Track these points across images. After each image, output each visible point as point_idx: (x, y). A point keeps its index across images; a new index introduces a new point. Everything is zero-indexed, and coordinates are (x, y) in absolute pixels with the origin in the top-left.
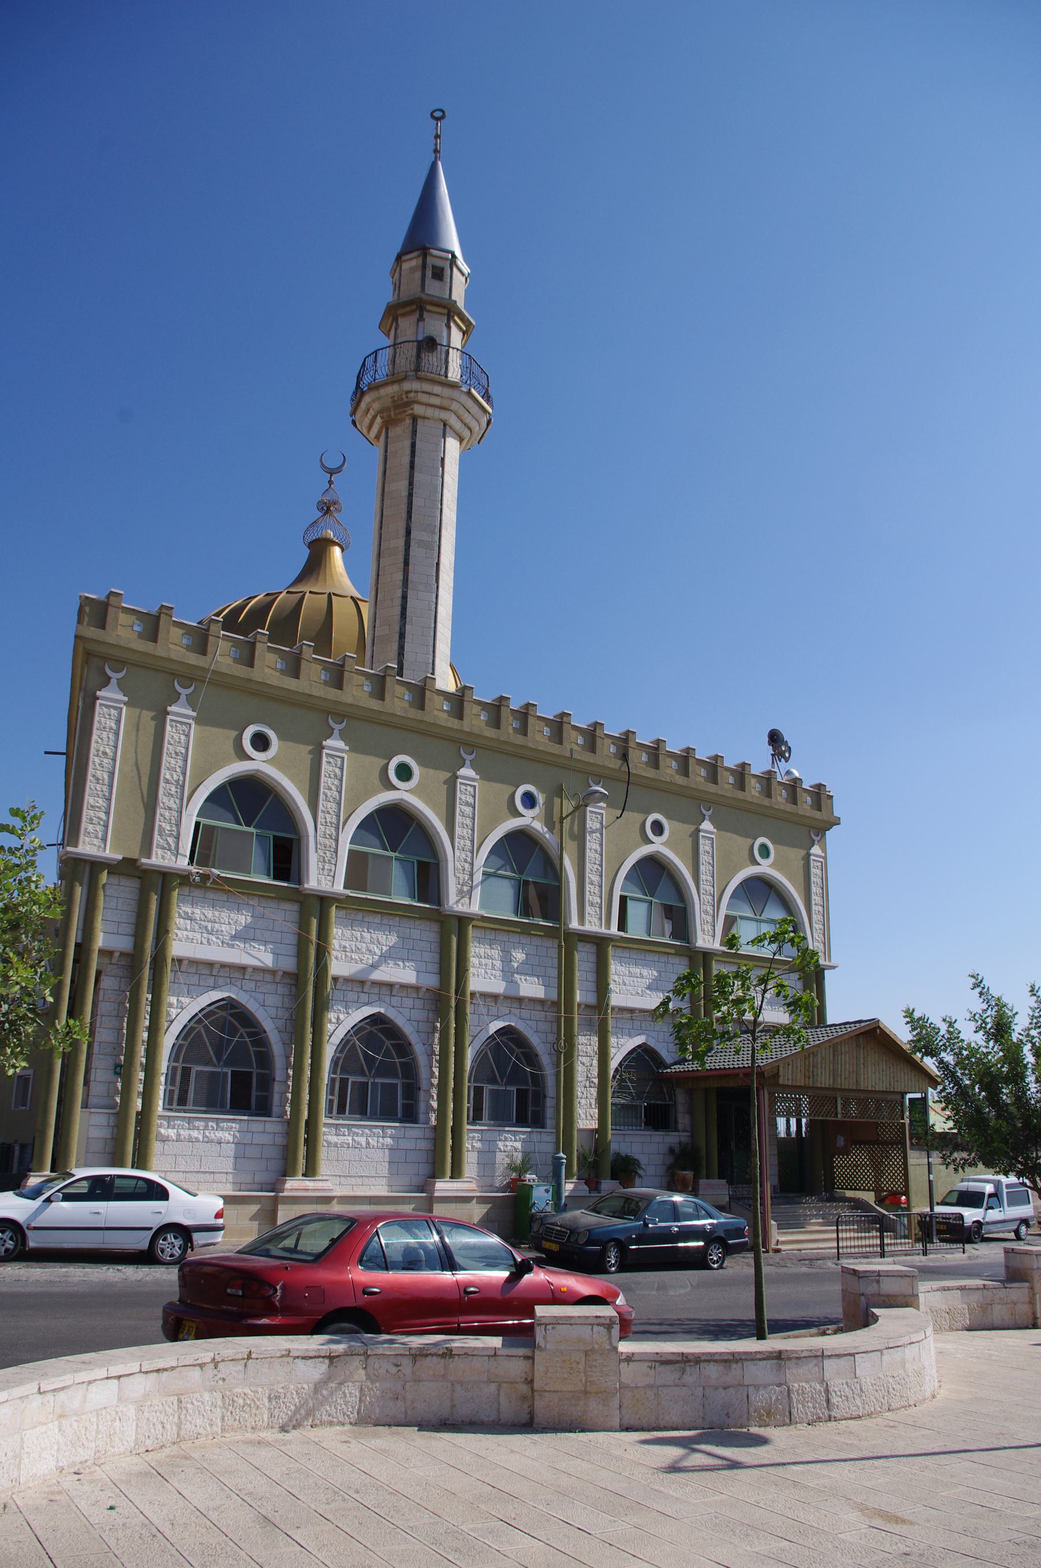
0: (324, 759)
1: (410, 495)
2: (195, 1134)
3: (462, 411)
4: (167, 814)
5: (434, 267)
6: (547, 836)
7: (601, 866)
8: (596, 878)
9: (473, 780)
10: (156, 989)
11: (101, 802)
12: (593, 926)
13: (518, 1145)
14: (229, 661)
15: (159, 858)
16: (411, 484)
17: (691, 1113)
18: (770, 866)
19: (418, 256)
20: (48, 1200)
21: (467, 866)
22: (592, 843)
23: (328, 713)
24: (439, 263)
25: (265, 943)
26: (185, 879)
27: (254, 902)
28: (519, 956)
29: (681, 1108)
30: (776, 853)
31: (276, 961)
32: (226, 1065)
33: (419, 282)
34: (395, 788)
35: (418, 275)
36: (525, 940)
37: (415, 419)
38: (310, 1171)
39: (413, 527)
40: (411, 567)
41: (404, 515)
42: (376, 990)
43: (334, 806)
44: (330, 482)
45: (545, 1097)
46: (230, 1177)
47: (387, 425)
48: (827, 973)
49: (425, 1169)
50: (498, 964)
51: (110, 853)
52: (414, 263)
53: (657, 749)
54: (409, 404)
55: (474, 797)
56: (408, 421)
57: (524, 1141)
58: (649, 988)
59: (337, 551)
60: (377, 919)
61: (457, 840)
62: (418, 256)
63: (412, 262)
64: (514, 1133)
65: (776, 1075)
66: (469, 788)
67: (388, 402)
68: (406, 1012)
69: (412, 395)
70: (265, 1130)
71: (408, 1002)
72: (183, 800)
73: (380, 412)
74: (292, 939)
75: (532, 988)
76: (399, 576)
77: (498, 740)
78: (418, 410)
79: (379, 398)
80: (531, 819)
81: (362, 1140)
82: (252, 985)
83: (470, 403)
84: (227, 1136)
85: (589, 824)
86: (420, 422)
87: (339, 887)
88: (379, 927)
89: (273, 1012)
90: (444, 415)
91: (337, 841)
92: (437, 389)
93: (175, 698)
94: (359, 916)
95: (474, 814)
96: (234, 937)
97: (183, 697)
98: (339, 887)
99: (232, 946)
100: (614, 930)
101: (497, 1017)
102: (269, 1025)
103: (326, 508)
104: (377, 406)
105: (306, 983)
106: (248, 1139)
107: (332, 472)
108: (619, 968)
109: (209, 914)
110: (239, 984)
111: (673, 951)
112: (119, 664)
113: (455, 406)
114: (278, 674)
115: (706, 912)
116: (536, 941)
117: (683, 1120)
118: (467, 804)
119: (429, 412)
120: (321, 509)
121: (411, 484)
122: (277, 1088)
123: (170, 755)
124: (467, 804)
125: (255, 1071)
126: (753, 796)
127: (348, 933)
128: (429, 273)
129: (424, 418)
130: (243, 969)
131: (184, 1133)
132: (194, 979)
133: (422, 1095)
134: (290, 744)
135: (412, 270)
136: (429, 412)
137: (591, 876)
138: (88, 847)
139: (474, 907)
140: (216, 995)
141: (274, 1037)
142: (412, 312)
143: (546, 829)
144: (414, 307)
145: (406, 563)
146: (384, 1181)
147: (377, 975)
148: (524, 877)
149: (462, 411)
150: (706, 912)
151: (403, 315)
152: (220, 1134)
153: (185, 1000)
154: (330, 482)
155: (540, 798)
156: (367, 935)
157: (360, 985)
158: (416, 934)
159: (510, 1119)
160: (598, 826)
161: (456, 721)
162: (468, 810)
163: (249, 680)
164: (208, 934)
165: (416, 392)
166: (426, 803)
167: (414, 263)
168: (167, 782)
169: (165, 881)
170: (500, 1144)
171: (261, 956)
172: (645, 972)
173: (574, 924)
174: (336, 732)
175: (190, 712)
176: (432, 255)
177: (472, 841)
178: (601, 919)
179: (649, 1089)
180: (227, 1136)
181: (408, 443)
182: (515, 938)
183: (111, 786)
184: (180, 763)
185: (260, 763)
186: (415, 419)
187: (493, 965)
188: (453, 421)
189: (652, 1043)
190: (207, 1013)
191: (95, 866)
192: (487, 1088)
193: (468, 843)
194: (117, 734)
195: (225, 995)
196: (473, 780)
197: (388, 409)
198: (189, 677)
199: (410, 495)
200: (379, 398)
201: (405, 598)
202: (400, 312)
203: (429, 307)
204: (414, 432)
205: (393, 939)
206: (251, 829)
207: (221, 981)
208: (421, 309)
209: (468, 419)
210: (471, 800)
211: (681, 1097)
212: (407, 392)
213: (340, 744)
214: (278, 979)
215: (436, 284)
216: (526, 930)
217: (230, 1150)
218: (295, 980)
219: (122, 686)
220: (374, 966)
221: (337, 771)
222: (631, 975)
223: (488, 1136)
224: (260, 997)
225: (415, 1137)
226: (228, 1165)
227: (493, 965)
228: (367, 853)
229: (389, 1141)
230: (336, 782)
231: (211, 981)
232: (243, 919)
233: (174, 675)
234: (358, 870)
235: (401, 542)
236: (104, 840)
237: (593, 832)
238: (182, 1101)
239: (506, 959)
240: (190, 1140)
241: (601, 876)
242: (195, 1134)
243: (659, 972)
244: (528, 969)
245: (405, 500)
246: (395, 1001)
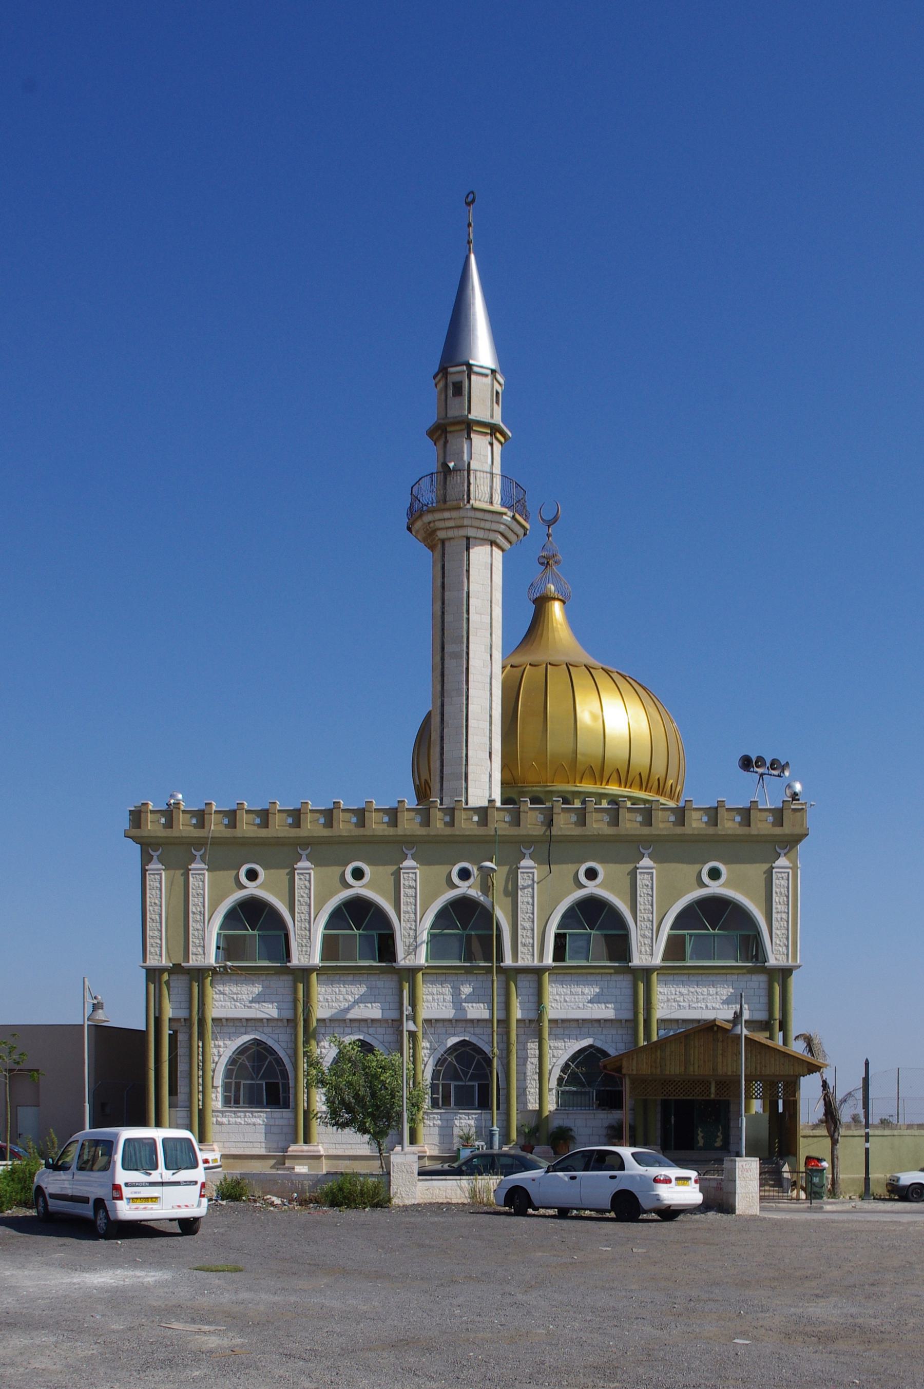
0: (297, 877)
2: (239, 1120)
3: (476, 523)
4: (196, 933)
6: (482, 898)
7: (533, 914)
8: (528, 925)
9: (414, 868)
10: (202, 1036)
11: (157, 933)
12: (525, 960)
13: (472, 1122)
14: (222, 828)
15: (194, 961)
16: (443, 603)
18: (723, 885)
19: (442, 377)
21: (412, 933)
22: (523, 898)
24: (456, 378)
26: (214, 970)
27: (263, 978)
28: (466, 990)
30: (728, 870)
31: (279, 1013)
32: (260, 1079)
34: (352, 887)
36: (471, 978)
37: (443, 542)
38: (307, 1141)
42: (357, 1024)
43: (306, 907)
46: (263, 1145)
50: (449, 998)
51: (165, 962)
54: (434, 532)
55: (416, 881)
56: (439, 546)
57: (476, 1119)
58: (590, 1002)
60: (350, 978)
61: (402, 915)
64: (468, 1114)
66: (411, 875)
68: (380, 1037)
69: (432, 525)
70: (281, 1115)
71: (381, 1030)
72: (205, 923)
74: (290, 998)
75: (477, 1011)
77: (428, 835)
78: (441, 535)
80: (470, 889)
82: (270, 1029)
83: (479, 515)
85: (521, 882)
86: (447, 544)
87: (316, 960)
88: (352, 983)
89: (284, 1045)
90: (462, 532)
91: (310, 931)
92: (447, 515)
93: (193, 859)
94: (337, 977)
95: (416, 893)
96: (251, 1002)
97: (198, 858)
98: (316, 960)
99: (251, 1007)
100: (549, 960)
101: (454, 1035)
102: (282, 1054)
105: (300, 1023)
106: (272, 1122)
109: (234, 990)
110: (261, 1030)
111: (612, 971)
113: (466, 522)
114: (256, 828)
115: (644, 936)
116: (480, 978)
118: (410, 887)
119: (450, 534)
121: (443, 603)
123: (194, 896)
124: (410, 887)
125: (280, 1081)
126: (694, 828)
127: (329, 990)
128: (450, 392)
129: (450, 539)
130: (261, 1020)
131: (233, 1120)
132: (233, 1030)
134: (272, 871)
136: (450, 534)
138: (152, 962)
139: (421, 959)
140: (246, 1038)
141: (286, 1060)
142: (441, 435)
143: (480, 894)
147: (350, 1016)
148: (468, 932)
149: (476, 523)
150: (644, 936)
152: (254, 1120)
153: (228, 1042)
155: (474, 870)
156: (343, 990)
157: (339, 1022)
158: (380, 984)
159: (473, 1104)
160: (530, 882)
161: (392, 829)
162: (411, 892)
164: (229, 1001)
165: (434, 521)
166: (377, 892)
168: (194, 913)
169: (199, 975)
170: (457, 1122)
171: (270, 1011)
172: (586, 991)
173: (508, 962)
174: (304, 857)
175: (203, 866)
177: (415, 914)
178: (533, 955)
179: (594, 1077)
182: (464, 978)
183: (161, 923)
184: (201, 900)
185: (253, 889)
187: (444, 1000)
188: (471, 532)
189: (598, 1044)
190: (242, 1050)
191: (161, 970)
192: (453, 1084)
193: (412, 916)
194: (161, 890)
195: (253, 1037)
196: (414, 868)
198: (199, 843)
199: (443, 613)
201: (443, 705)
205: (363, 989)
206: (256, 932)
207: (249, 1029)
209: (488, 525)
210: (412, 883)
212: (430, 523)
213: (307, 864)
216: (468, 971)
217: (262, 1129)
219: (161, 861)
220: (348, 1009)
221: (307, 883)
222: (572, 994)
223: (445, 1116)
224: (275, 1037)
226: (262, 1138)
227: (444, 1000)
228: (338, 935)
230: (307, 891)
231: (243, 1030)
232: (257, 989)
234: (330, 948)
236: (161, 955)
237: (524, 888)
238: (237, 1102)
239: (456, 993)
240: (236, 1123)
241: (533, 922)
242: (239, 1120)
243: (602, 989)
244: (474, 998)
246: (371, 1030)
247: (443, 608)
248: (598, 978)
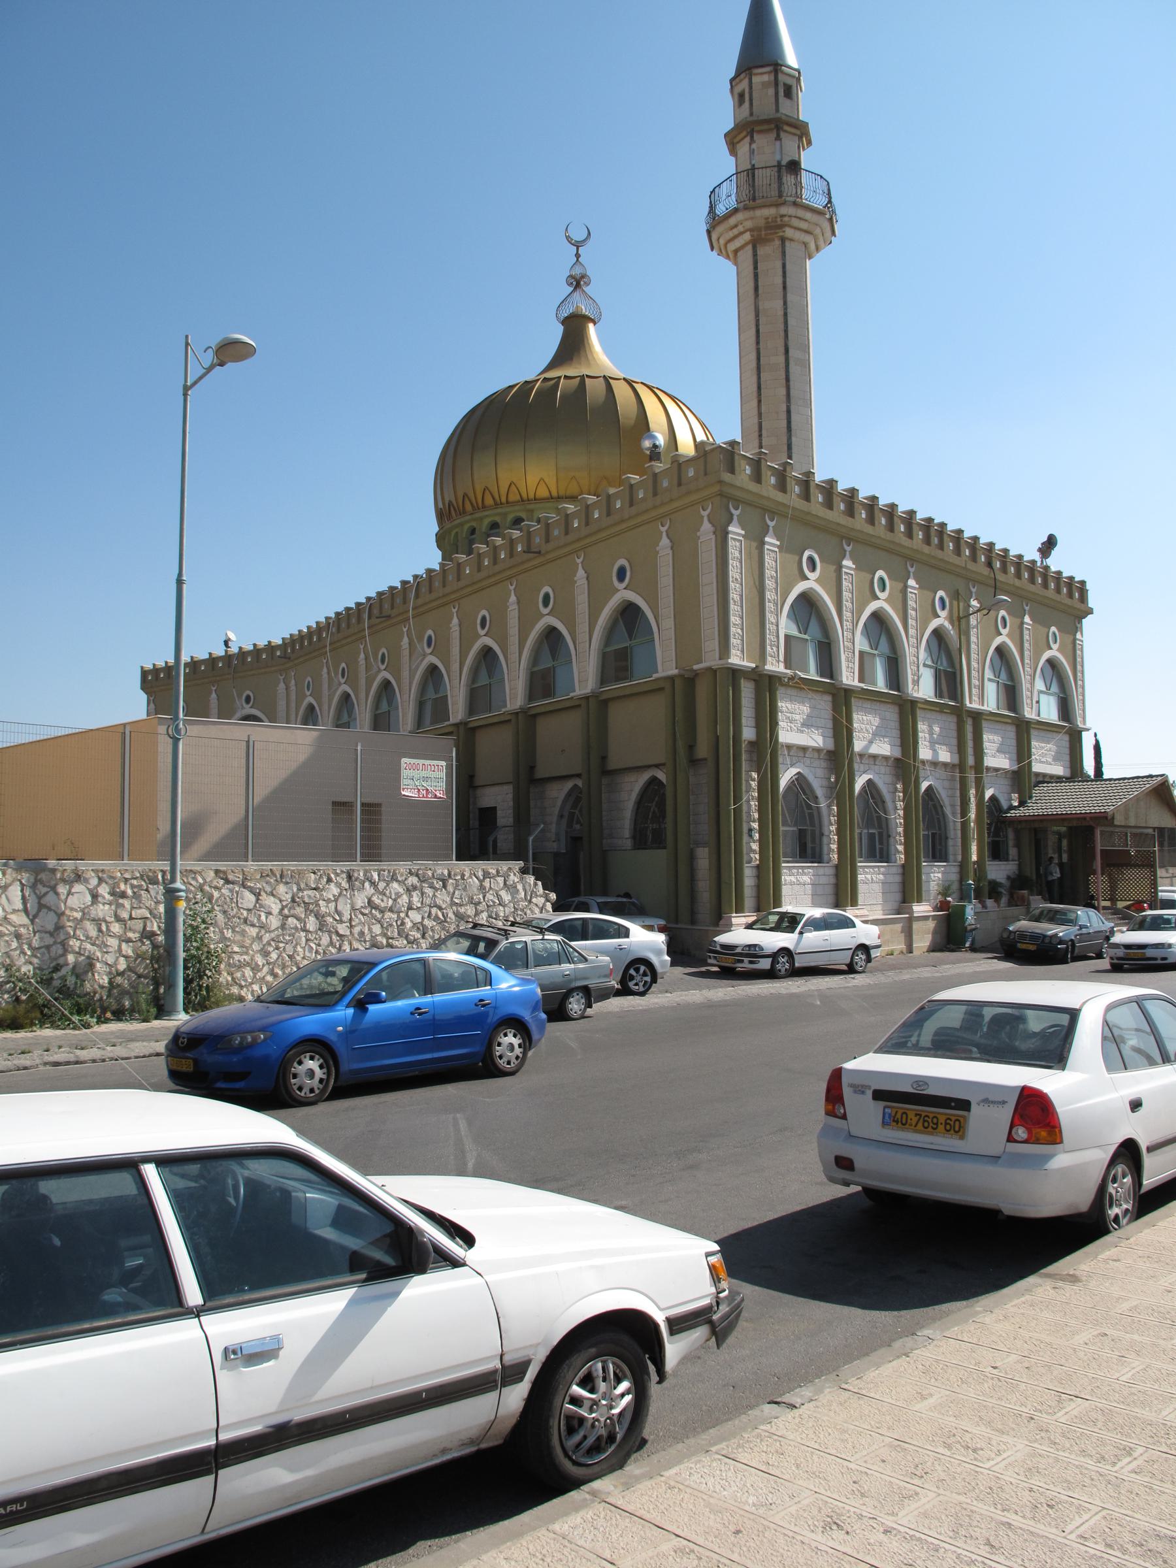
1: (785, 315)
5: (785, 84)
16: (785, 303)
17: (1018, 845)
19: (769, 73)
20: (801, 933)
23: (842, 537)
24: (790, 81)
25: (817, 728)
29: (1011, 843)
31: (824, 742)
33: (773, 100)
35: (771, 91)
36: (939, 716)
37: (783, 240)
39: (790, 344)
40: (791, 383)
41: (782, 334)
44: (578, 256)
45: (947, 838)
47: (755, 243)
48: (1084, 733)
49: (898, 897)
52: (766, 78)
53: (1004, 557)
54: (782, 226)
56: (777, 242)
57: (943, 873)
59: (591, 326)
62: (769, 73)
63: (762, 78)
65: (1113, 818)
67: (762, 223)
69: (786, 219)
73: (750, 230)
76: (783, 391)
78: (789, 233)
79: (752, 218)
81: (869, 876)
84: (806, 879)
86: (787, 244)
99: (802, 732)
103: (577, 282)
104: (749, 224)
107: (578, 245)
108: (991, 737)
112: (738, 502)
117: (1013, 852)
119: (798, 235)
120: (570, 284)
121: (785, 303)
122: (950, 842)
128: (781, 93)
129: (791, 240)
133: (825, 840)
135: (765, 85)
137: (974, 664)
144: (773, 126)
145: (788, 380)
146: (880, 907)
151: (760, 132)
154: (578, 256)
163: (809, 513)
167: (766, 78)
176: (783, 72)
180: (806, 879)
181: (779, 264)
186: (783, 240)
197: (759, 229)
199: (785, 315)
200: (752, 218)
201: (789, 412)
202: (756, 128)
203: (786, 128)
204: (784, 253)
206: (806, 637)
208: (778, 129)
211: (1011, 835)
212: (782, 216)
214: (822, 756)
215: (788, 102)
218: (961, 766)
225: (825, 872)
229: (881, 877)
233: (765, 510)
235: (782, 359)
245: (782, 319)
247: (786, 309)
248: (998, 726)
